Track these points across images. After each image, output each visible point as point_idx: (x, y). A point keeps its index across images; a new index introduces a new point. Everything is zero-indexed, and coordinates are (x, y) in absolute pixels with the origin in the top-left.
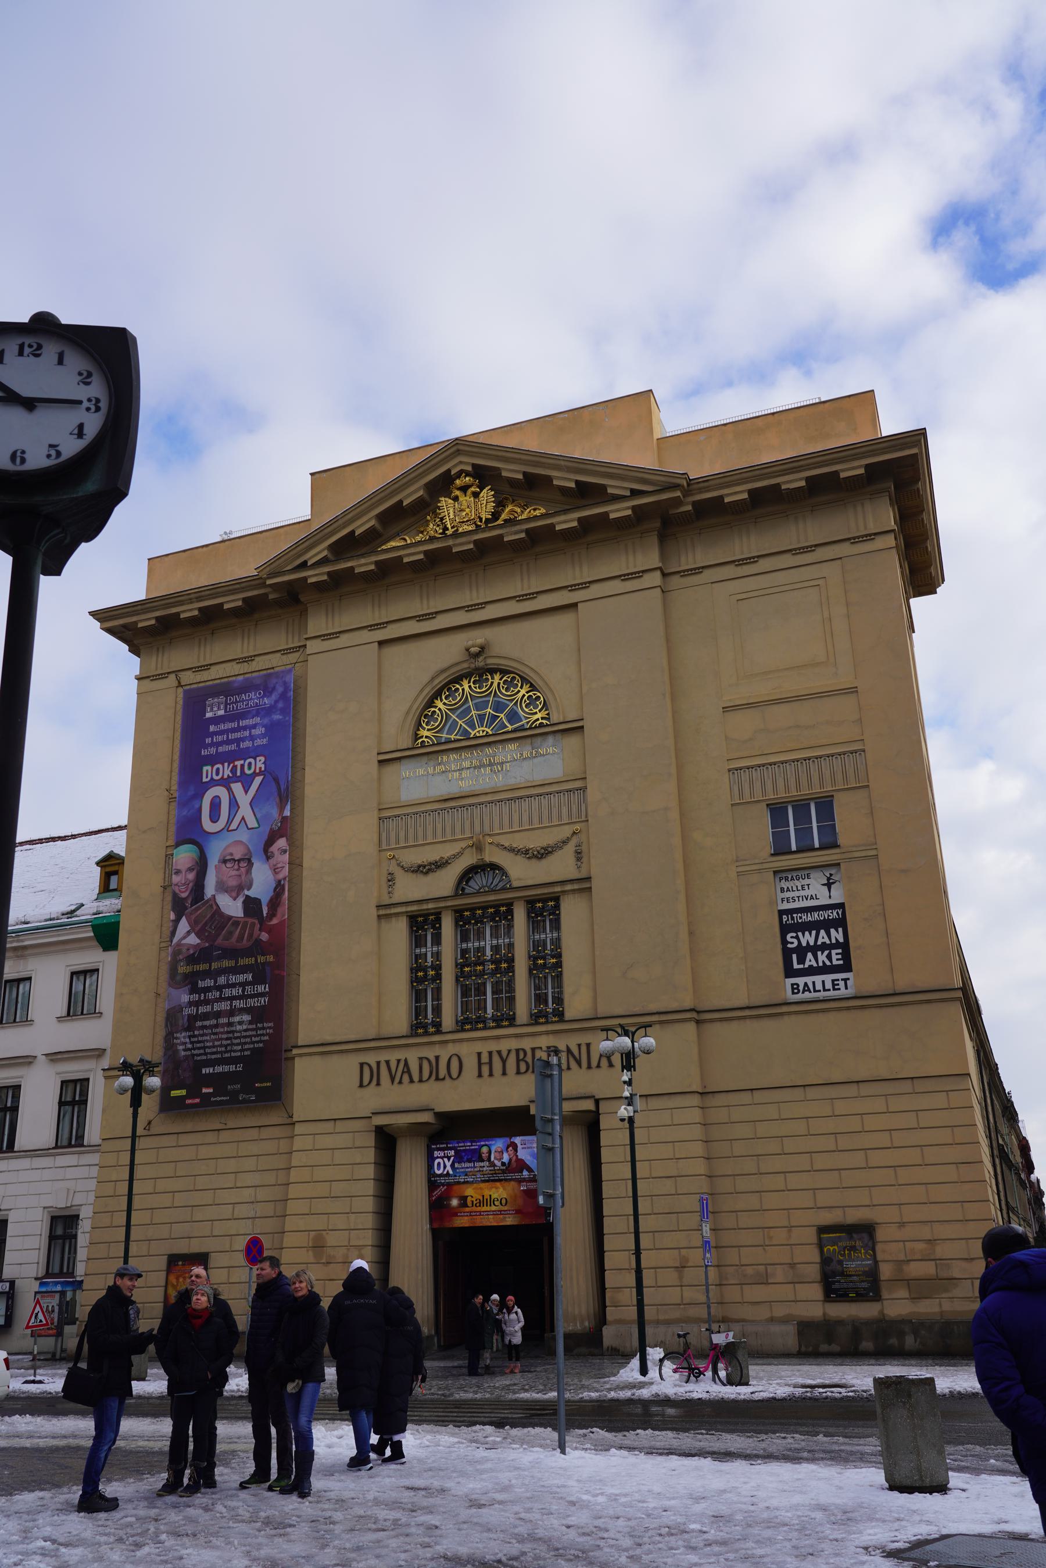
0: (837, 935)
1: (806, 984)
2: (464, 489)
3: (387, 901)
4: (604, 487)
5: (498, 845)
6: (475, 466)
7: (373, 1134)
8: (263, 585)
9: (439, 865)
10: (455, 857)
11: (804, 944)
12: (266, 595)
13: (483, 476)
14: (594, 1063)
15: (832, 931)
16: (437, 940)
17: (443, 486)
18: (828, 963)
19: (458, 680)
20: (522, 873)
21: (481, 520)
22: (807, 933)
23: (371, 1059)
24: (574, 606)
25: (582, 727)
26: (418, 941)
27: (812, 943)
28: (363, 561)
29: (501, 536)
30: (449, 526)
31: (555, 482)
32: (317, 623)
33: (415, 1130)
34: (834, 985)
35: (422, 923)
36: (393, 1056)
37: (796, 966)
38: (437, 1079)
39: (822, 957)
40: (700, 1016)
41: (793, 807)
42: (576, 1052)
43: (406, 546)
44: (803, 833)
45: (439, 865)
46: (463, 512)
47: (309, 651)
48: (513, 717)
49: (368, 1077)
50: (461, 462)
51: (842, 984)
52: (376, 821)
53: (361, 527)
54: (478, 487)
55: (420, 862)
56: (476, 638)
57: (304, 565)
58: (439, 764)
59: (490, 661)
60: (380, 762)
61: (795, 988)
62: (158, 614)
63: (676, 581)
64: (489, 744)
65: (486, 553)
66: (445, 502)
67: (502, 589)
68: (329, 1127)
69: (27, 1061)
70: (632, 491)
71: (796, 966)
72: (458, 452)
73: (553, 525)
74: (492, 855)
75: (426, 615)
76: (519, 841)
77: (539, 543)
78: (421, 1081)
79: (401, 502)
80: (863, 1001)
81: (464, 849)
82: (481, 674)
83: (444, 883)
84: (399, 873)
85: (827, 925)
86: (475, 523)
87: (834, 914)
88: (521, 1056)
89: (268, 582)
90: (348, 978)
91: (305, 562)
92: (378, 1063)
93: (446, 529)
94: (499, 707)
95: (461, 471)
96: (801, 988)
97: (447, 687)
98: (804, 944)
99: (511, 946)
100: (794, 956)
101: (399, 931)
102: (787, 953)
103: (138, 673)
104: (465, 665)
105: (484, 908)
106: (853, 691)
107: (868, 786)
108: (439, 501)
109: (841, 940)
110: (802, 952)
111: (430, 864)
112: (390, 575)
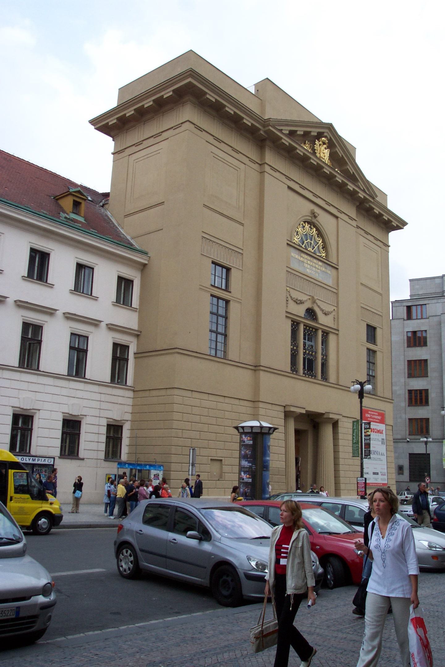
4: (357, 180)
9: (301, 302)
13: (331, 145)
24: (337, 217)
56: (317, 210)
60: (288, 244)
82: (312, 224)
84: (289, 299)
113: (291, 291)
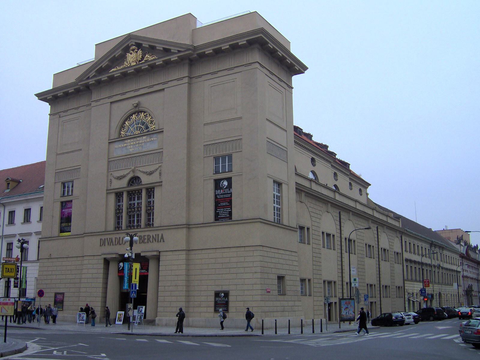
2: (133, 50)
3: (109, 188)
7: (103, 260)
8: (78, 85)
9: (124, 177)
10: (128, 174)
12: (80, 88)
13: (139, 46)
14: (159, 241)
17: (127, 50)
19: (132, 115)
20: (145, 180)
23: (103, 237)
24: (163, 89)
28: (104, 76)
32: (95, 97)
33: (113, 259)
35: (119, 195)
36: (108, 237)
38: (119, 244)
40: (188, 226)
42: (155, 236)
43: (115, 71)
44: (224, 167)
45: (124, 177)
47: (92, 105)
48: (147, 127)
49: (103, 243)
50: (131, 42)
52: (106, 163)
53: (104, 64)
54: (137, 49)
55: (118, 176)
56: (135, 101)
57: (88, 78)
58: (125, 143)
59: (140, 109)
60: (109, 142)
62: (52, 94)
63: (194, 80)
64: (138, 137)
65: (138, 73)
67: (144, 84)
68: (92, 257)
69: (30, 234)
72: (131, 39)
73: (155, 63)
77: (153, 69)
78: (115, 245)
79: (115, 56)
81: (130, 172)
82: (139, 112)
83: (124, 183)
88: (141, 237)
89: (79, 84)
91: (89, 77)
92: (105, 239)
94: (143, 124)
95: (132, 45)
97: (128, 118)
99: (141, 203)
101: (112, 198)
103: (49, 113)
104: (133, 110)
105: (135, 191)
106: (240, 118)
111: (121, 176)
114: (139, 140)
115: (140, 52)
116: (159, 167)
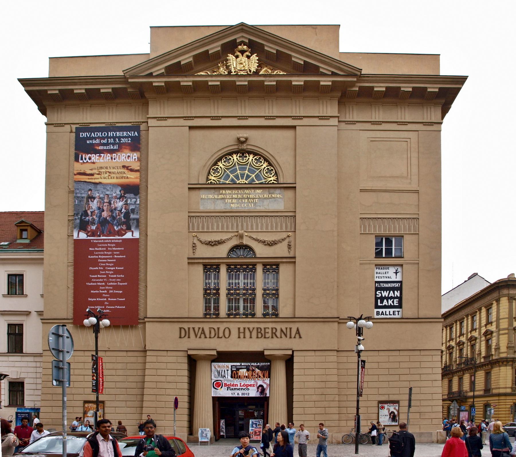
0: (397, 294)
1: (382, 312)
5: (250, 237)
6: (249, 40)
9: (220, 243)
11: (384, 296)
13: (254, 48)
15: (396, 292)
16: (217, 277)
17: (231, 47)
18: (392, 304)
20: (261, 251)
21: (250, 71)
22: (385, 292)
25: (295, 187)
26: (207, 277)
27: (387, 296)
29: (263, 82)
30: (233, 71)
31: (293, 59)
34: (394, 313)
37: (379, 304)
39: (390, 302)
41: (385, 238)
45: (220, 243)
46: (243, 64)
50: (243, 37)
51: (397, 313)
54: (250, 53)
55: (210, 240)
56: (243, 134)
61: (378, 313)
65: (253, 90)
66: (231, 57)
70: (332, 72)
71: (379, 304)
72: (242, 30)
74: (246, 241)
75: (216, 117)
76: (261, 237)
80: (404, 320)
81: (233, 237)
83: (222, 251)
85: (394, 289)
86: (247, 72)
87: (397, 285)
90: (170, 286)
93: (230, 72)
96: (380, 313)
98: (384, 296)
100: (379, 300)
102: (376, 299)
107: (418, 234)
108: (228, 56)
109: (399, 296)
110: (382, 299)
111: (215, 241)
112: (201, 92)
113: (199, 235)
114: (249, 194)
115: (254, 58)
116: (288, 236)
